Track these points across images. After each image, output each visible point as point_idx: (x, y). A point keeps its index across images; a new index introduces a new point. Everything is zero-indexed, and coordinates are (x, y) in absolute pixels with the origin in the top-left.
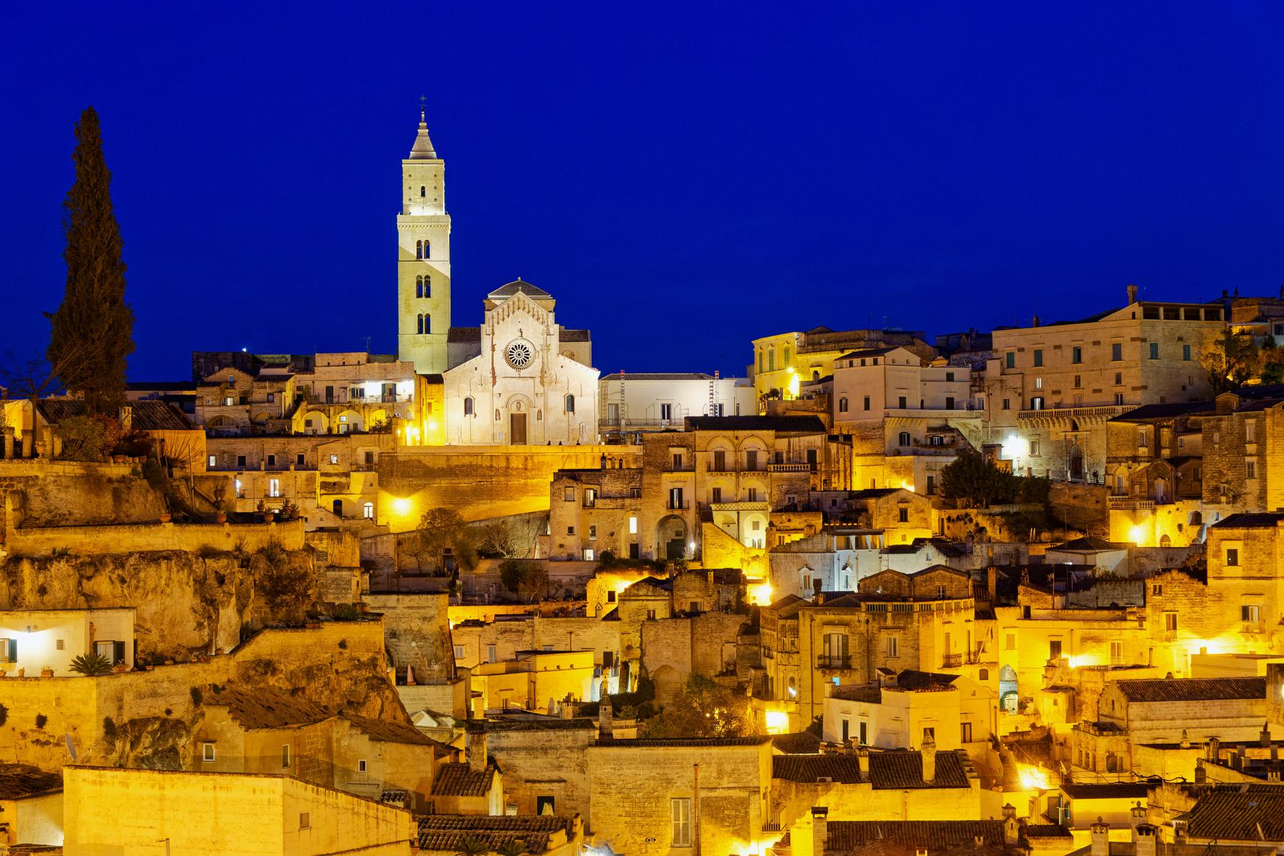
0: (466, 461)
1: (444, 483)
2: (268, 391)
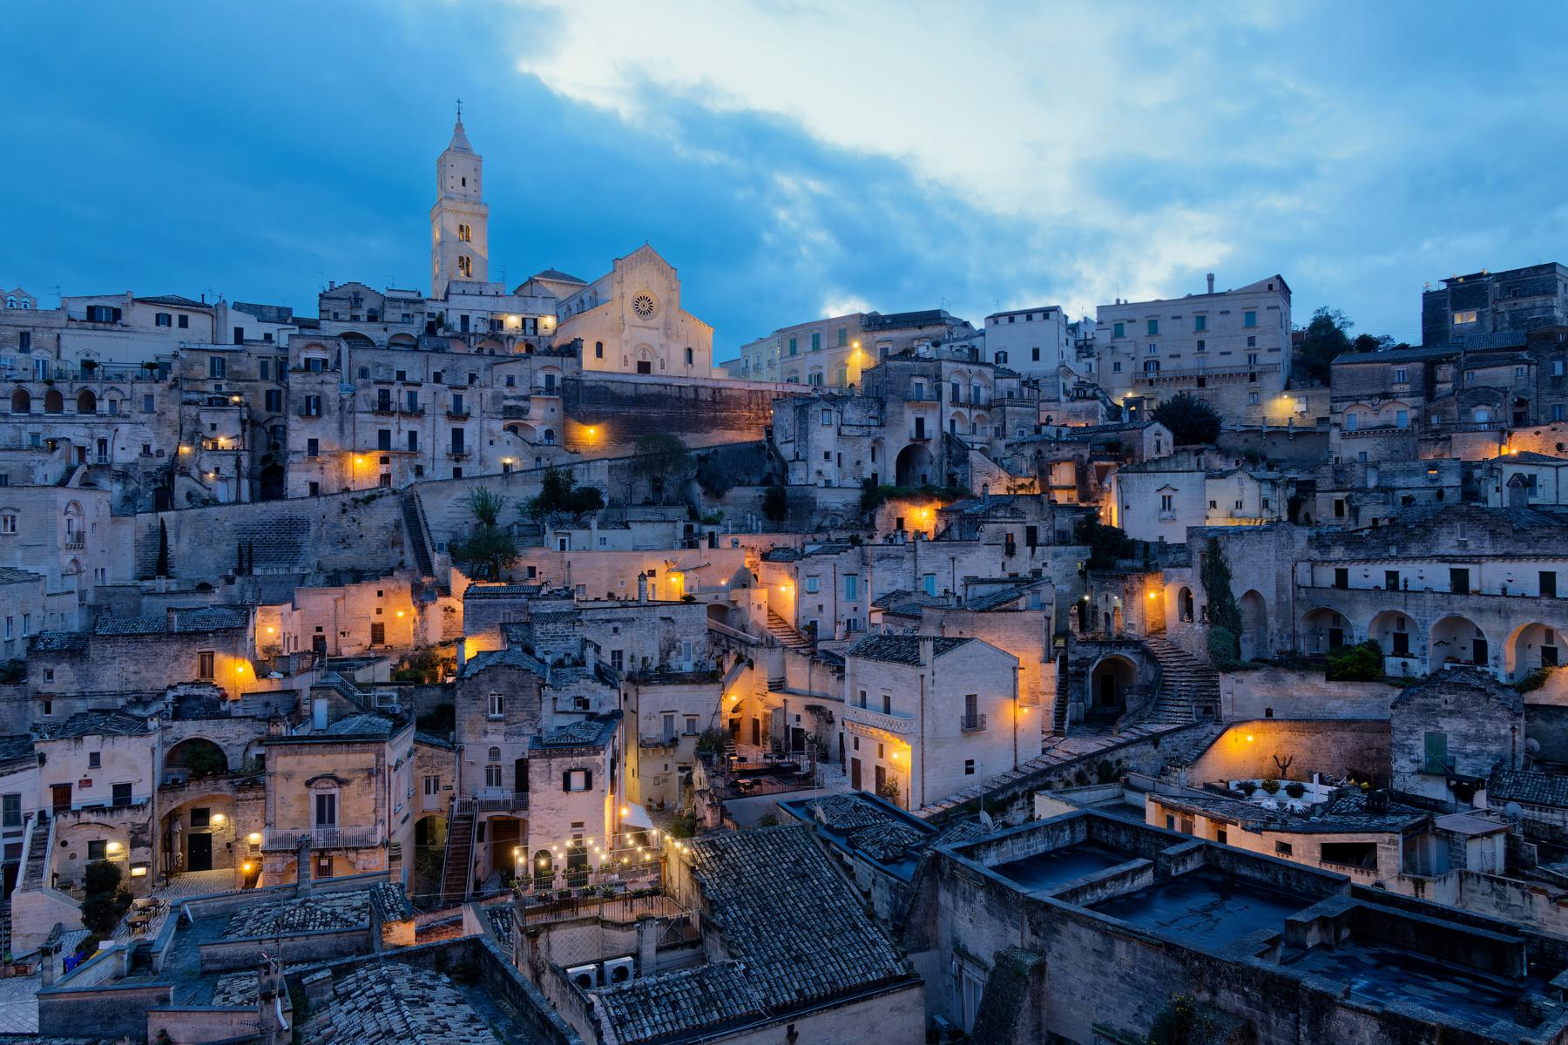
0: (656, 389)
2: (403, 311)
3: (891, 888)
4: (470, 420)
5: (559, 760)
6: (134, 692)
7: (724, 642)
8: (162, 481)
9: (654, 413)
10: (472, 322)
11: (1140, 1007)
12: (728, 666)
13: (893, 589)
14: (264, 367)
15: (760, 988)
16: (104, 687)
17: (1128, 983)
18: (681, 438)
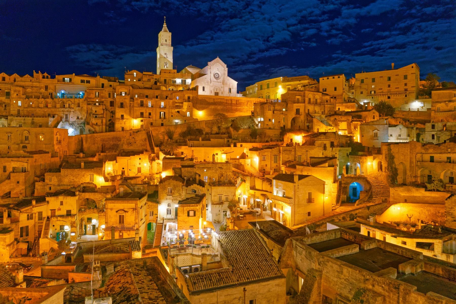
1: (213, 107)
2: (148, 78)
3: (279, 249)
4: (166, 109)
5: (186, 207)
6: (73, 185)
7: (237, 175)
8: (82, 127)
9: (219, 107)
10: (167, 81)
11: (350, 289)
12: (239, 181)
13: (288, 160)
14: (109, 94)
15: (236, 277)
16: (65, 183)
17: (347, 282)
18: (226, 115)
